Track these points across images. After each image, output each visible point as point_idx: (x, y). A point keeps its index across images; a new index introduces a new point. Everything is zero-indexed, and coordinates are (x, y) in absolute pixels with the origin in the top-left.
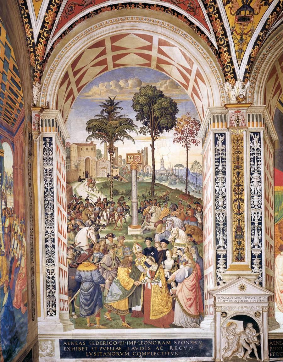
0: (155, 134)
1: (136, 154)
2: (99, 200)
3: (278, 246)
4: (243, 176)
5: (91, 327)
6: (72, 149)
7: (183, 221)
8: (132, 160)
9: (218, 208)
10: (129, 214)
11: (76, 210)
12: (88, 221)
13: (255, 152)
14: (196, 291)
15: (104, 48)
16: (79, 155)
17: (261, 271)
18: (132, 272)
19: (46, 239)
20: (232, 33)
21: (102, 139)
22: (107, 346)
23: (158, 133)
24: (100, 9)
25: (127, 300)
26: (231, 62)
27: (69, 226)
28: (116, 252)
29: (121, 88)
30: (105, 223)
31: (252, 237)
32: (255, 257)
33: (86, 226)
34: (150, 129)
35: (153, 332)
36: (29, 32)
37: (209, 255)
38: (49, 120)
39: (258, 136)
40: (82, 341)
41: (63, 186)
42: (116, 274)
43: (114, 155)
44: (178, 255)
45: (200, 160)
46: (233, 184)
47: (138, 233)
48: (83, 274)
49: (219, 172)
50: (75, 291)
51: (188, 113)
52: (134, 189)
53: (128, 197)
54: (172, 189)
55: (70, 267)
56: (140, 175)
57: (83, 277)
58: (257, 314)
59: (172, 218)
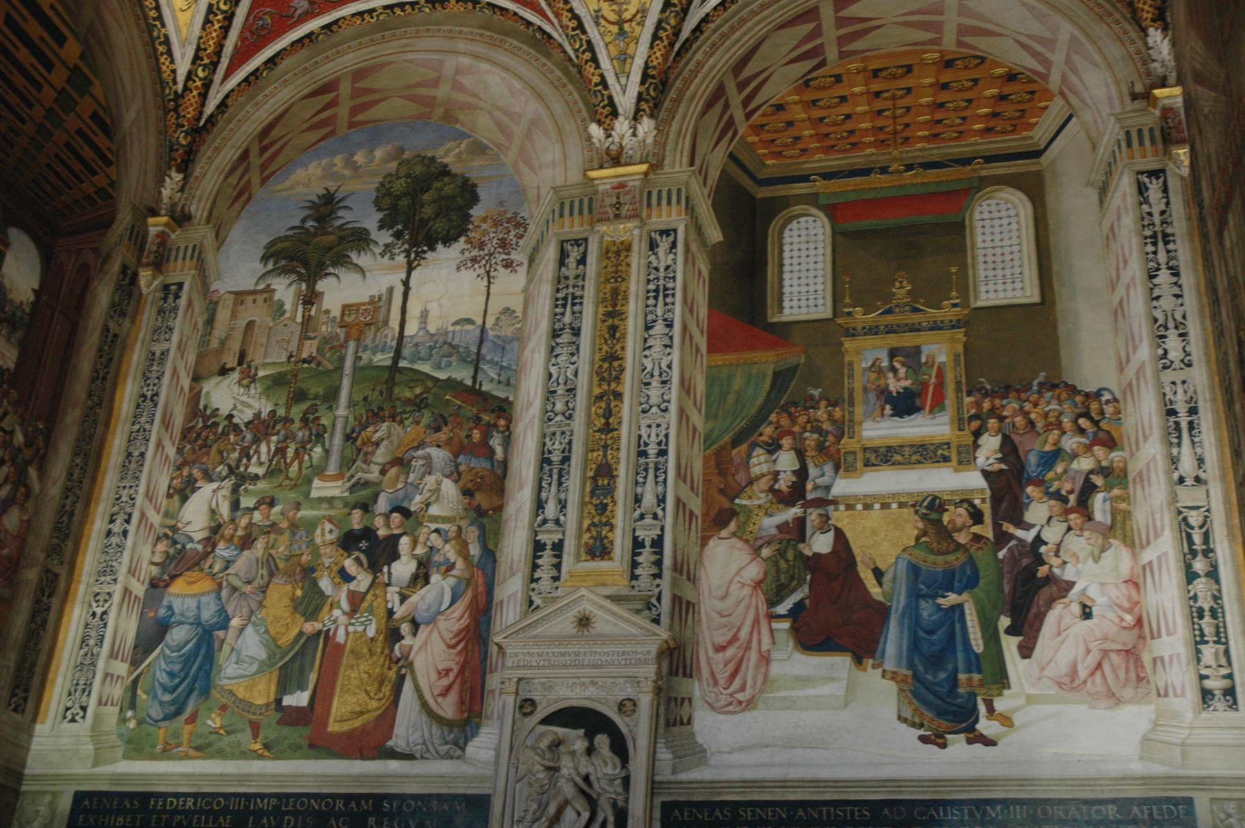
0: (417, 254)
1: (364, 304)
2: (257, 415)
3: (713, 513)
4: (624, 336)
5: (166, 753)
6: (221, 303)
7: (456, 456)
8: (353, 317)
9: (550, 420)
10: (323, 445)
11: (200, 442)
12: (218, 469)
13: (662, 274)
14: (465, 647)
15: (333, 95)
16: (234, 315)
17: (658, 586)
18: (304, 596)
19: (112, 515)
20: (597, 24)
21: (293, 277)
22: (195, 812)
23: (424, 252)
24: (336, 22)
25: (276, 674)
26: (604, 83)
27: (175, 482)
28: (271, 542)
29: (355, 167)
30: (260, 471)
31: (639, 490)
32: (644, 547)
33: (212, 481)
34: (406, 246)
35: (327, 771)
36: (168, 72)
37: (515, 545)
38: (186, 248)
39: (671, 239)
40: (132, 795)
41: (182, 389)
42: (261, 605)
43: (314, 309)
44: (431, 548)
45: (517, 304)
46: (597, 357)
47: (336, 493)
48: (177, 605)
49: (562, 329)
50: (148, 651)
51: (501, 203)
52: (346, 383)
53: (327, 405)
54: (437, 380)
55: (154, 584)
56: (365, 350)
57: (177, 611)
58: (627, 706)
59: (428, 450)
